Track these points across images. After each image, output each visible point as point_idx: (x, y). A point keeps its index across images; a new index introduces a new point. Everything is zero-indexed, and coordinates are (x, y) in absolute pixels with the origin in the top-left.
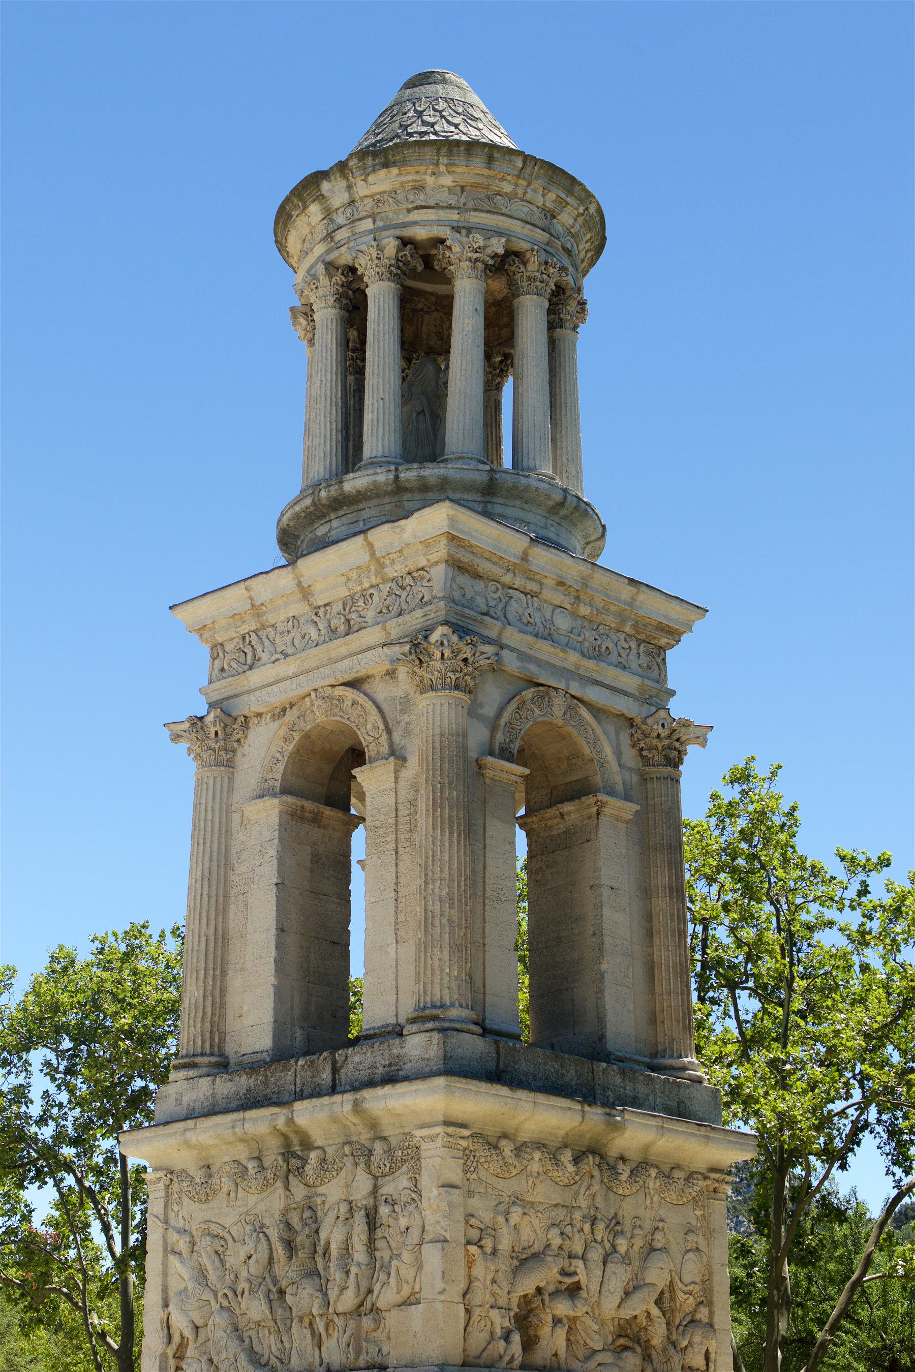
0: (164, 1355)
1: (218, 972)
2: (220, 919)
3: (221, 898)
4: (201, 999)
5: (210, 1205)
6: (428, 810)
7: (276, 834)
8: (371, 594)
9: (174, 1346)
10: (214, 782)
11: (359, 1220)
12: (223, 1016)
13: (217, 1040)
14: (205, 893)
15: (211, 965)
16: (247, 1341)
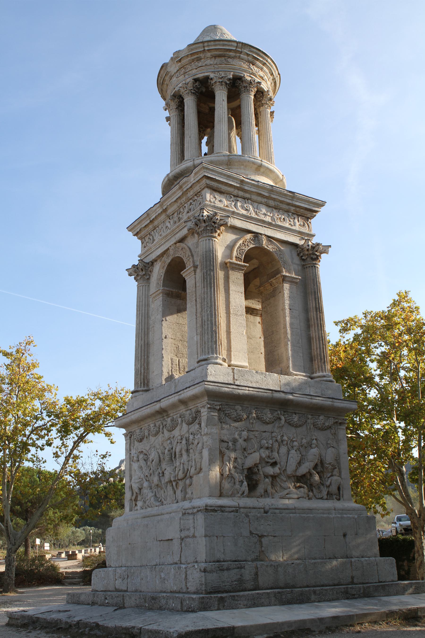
0: (131, 500)
1: (146, 357)
2: (146, 337)
3: (146, 330)
4: (140, 368)
5: (142, 443)
6: (202, 281)
7: (161, 302)
8: (185, 207)
9: (134, 497)
10: (143, 288)
11: (184, 442)
12: (148, 373)
13: (146, 382)
14: (140, 328)
15: (143, 354)
16: (154, 493)
